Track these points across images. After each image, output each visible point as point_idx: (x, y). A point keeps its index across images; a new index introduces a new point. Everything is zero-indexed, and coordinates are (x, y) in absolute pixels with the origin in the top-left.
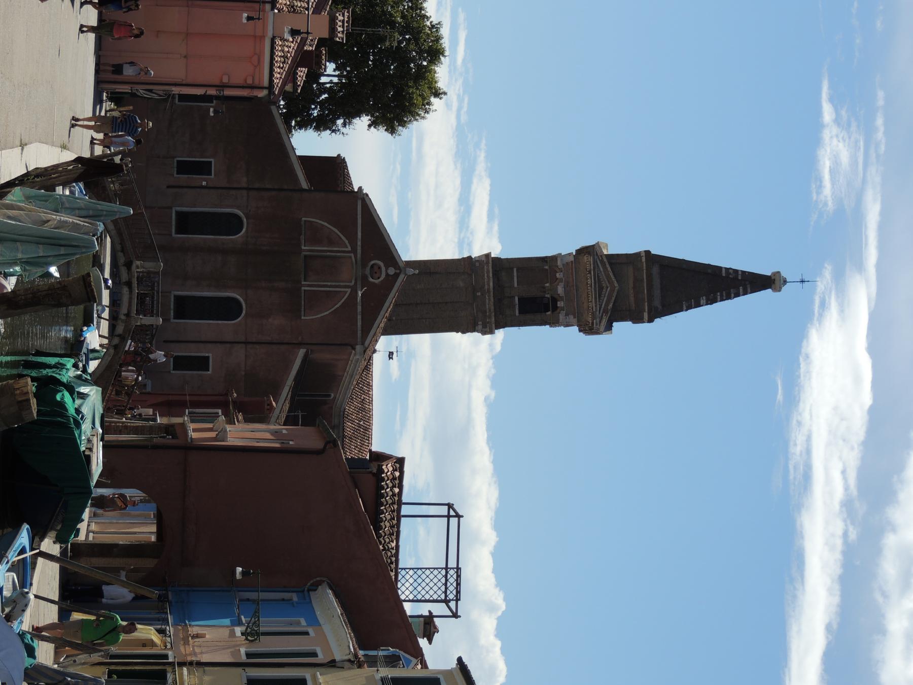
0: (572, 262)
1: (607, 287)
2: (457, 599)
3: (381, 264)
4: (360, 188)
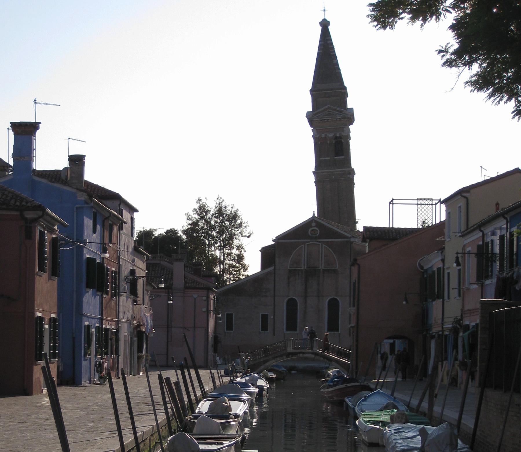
0: (316, 130)
1: (329, 111)
2: (432, 200)
3: (310, 229)
4: (273, 241)
